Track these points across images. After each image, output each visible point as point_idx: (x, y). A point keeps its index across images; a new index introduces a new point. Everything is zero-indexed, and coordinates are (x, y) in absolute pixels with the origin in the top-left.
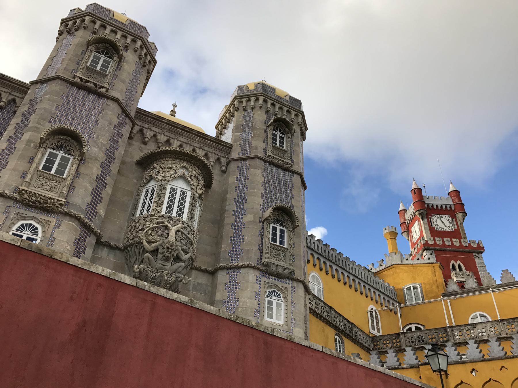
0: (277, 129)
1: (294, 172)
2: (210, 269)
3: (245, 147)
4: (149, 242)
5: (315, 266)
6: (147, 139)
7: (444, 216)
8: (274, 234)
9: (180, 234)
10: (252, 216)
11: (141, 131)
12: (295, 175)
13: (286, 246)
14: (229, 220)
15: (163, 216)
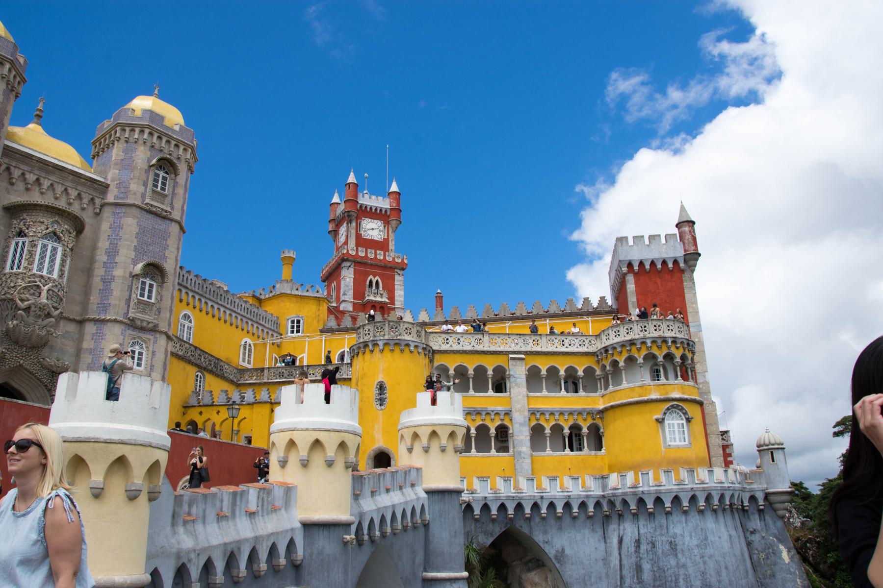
0: (161, 167)
1: (172, 220)
2: (78, 318)
3: (122, 190)
4: (22, 300)
5: (188, 304)
6: (14, 181)
7: (376, 221)
8: (143, 289)
9: (51, 292)
10: (122, 271)
11: (8, 169)
12: (173, 223)
13: (153, 301)
14: (99, 271)
15: (34, 275)
